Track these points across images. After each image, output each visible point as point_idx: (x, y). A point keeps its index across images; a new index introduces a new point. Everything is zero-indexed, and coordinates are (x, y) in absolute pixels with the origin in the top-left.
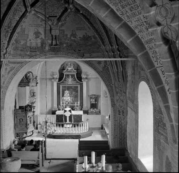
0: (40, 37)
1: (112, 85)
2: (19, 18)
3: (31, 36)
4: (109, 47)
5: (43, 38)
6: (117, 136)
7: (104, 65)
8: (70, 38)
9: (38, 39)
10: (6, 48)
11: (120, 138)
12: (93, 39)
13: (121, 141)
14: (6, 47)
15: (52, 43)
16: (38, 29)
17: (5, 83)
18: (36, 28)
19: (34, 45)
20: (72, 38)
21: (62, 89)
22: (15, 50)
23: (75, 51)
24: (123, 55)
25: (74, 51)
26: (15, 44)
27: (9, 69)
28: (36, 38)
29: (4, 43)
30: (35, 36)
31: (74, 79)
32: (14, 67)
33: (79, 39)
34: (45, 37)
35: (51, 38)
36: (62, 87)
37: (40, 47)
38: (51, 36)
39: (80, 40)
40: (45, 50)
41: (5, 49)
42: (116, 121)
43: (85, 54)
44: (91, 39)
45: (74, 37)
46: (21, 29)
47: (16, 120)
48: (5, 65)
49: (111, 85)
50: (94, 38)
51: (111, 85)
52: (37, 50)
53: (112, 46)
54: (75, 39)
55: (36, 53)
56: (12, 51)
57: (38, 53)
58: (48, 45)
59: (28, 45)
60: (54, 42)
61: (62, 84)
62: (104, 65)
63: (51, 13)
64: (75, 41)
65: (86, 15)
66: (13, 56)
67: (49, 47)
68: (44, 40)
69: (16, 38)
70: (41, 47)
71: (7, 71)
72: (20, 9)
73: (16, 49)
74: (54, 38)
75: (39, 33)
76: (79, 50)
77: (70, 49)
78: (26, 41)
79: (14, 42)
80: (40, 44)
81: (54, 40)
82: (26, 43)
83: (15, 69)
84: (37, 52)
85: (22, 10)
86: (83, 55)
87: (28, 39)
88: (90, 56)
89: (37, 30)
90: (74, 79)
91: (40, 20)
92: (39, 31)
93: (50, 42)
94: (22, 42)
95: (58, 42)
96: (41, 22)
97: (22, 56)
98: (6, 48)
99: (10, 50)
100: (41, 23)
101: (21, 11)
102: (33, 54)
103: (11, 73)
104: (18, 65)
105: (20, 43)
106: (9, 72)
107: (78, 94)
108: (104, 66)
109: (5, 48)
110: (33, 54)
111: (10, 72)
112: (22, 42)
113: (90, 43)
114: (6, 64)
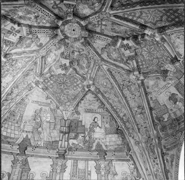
0: (179, 100)
2: (138, 92)
3: (170, 105)
9: (178, 103)
18: (166, 92)
22: (163, 131)
26: (159, 124)
28: (175, 103)
30: (171, 101)
46: (153, 102)
56: (161, 134)
59: (173, 116)
63: (159, 62)
65: (177, 20)
72: (131, 83)
75: (173, 94)
82: (170, 115)
85: (134, 83)
91: (161, 80)
94: (166, 117)
96: (165, 81)
100: (165, 83)
101: (135, 84)
105: (164, 119)
112: (166, 117)
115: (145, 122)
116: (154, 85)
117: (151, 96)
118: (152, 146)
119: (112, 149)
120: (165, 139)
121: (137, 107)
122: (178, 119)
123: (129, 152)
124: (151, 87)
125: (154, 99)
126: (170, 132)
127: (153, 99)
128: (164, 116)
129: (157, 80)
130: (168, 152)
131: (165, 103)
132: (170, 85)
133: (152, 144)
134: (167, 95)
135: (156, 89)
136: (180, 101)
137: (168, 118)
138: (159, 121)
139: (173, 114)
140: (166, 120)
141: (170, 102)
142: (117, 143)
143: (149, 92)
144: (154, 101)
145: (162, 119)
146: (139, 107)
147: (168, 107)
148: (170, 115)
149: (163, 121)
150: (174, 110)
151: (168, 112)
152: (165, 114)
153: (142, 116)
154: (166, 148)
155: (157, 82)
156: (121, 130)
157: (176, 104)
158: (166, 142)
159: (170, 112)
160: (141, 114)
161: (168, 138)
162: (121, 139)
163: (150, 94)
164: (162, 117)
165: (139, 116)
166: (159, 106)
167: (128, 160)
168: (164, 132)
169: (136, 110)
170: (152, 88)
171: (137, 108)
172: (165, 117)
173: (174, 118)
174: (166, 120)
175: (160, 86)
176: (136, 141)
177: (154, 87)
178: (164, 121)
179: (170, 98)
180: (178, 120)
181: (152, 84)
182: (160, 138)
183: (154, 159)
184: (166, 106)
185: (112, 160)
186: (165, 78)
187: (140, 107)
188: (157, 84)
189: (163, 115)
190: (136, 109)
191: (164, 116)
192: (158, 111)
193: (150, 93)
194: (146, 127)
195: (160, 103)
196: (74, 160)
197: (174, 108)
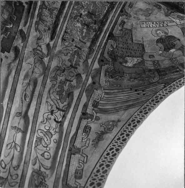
16: (167, 31)
28: (167, 49)
46: (121, 30)
78: (140, 59)
82: (143, 62)
89: (163, 32)
91: (162, 11)
92: (169, 34)
96: (167, 15)
98: (86, 61)
105: (126, 62)
116: (144, 11)
117: (126, 20)
118: (67, 85)
120: (107, 91)
121: (88, 12)
124: (135, 10)
125: (128, 26)
127: (125, 26)
129: (154, 8)
130: (98, 115)
131: (145, 44)
132: (174, 24)
134: (157, 34)
135: (143, 18)
143: (128, 13)
144: (124, 30)
146: (90, 14)
147: (148, 50)
149: (121, 63)
151: (142, 57)
153: (85, 30)
154: (99, 107)
155: (152, 10)
156: (24, 7)
159: (146, 58)
160: (86, 27)
161: (116, 91)
162: (6, 17)
163: (127, 16)
164: (123, 57)
165: (79, 25)
166: (130, 42)
169: (83, 14)
170: (136, 11)
171: (86, 13)
175: (152, 17)
177: (141, 13)
179: (160, 40)
181: (142, 8)
182: (97, 84)
183: (54, 108)
186: (171, 12)
187: (93, 17)
188: (150, 12)
189: (128, 56)
190: (84, 12)
192: (121, 46)
193: (128, 16)
195: (134, 39)
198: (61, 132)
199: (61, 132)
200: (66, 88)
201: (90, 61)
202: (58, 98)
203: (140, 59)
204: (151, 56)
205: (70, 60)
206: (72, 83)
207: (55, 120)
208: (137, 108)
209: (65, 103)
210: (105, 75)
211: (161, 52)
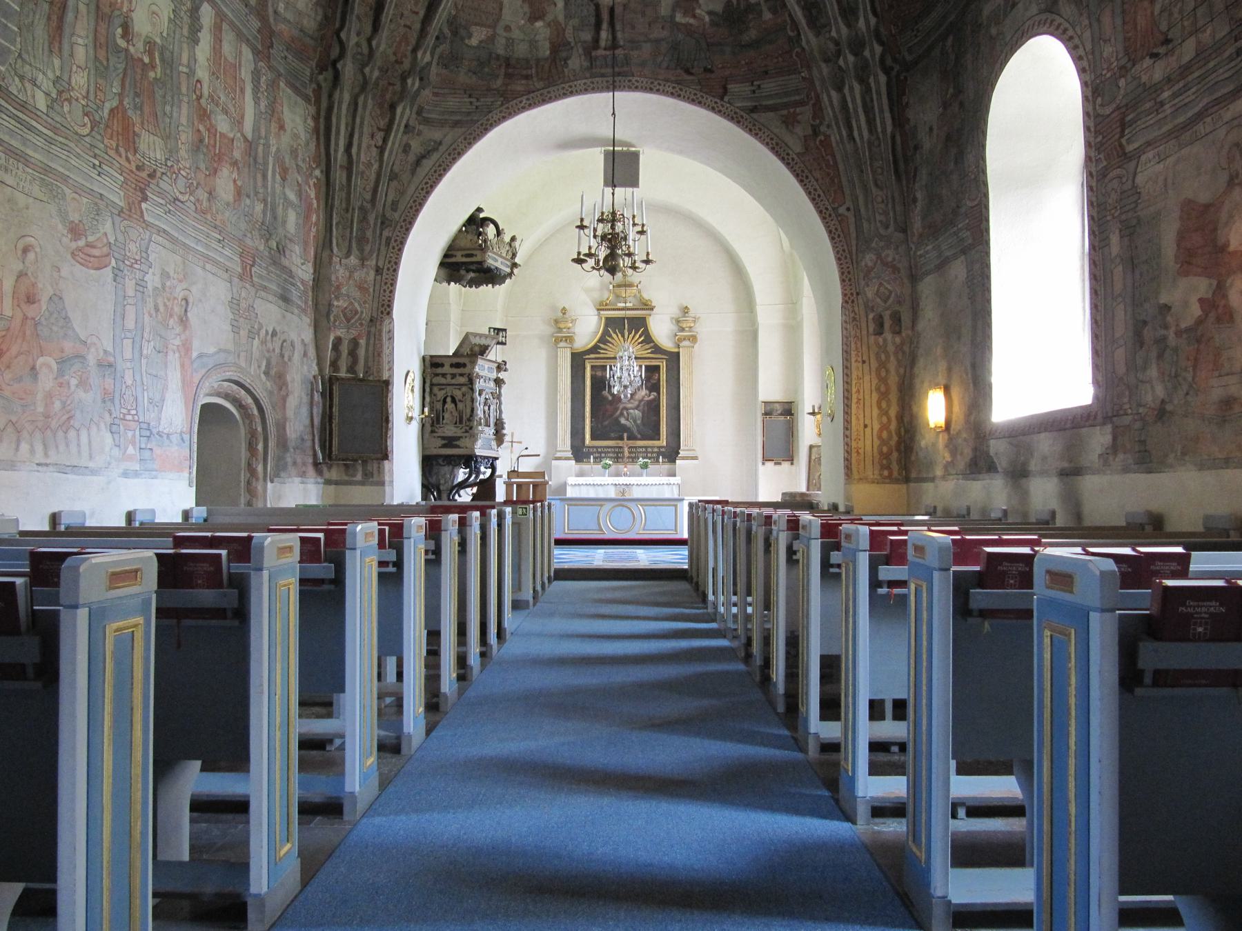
0: (549, 18)
1: (846, 213)
4: (838, 31)
5: (561, 18)
6: (868, 430)
7: (812, 125)
8: (672, 17)
9: (539, 24)
10: (415, 51)
11: (880, 437)
12: (767, 15)
13: (885, 449)
14: (413, 41)
15: (596, 40)
17: (401, 207)
19: (521, 50)
20: (679, 18)
21: (593, 377)
22: (446, 66)
23: (691, 74)
24: (895, 60)
25: (688, 72)
27: (416, 146)
29: (405, 26)
31: (642, 338)
32: (440, 143)
33: (707, 19)
34: (568, 16)
35: (593, 20)
36: (592, 367)
37: (546, 59)
38: (592, 8)
39: (714, 24)
40: (565, 70)
41: (409, 54)
42: (864, 362)
43: (729, 86)
44: (760, 13)
45: (685, 14)
47: (428, 399)
48: (402, 129)
49: (842, 210)
50: (769, 9)
51: (842, 210)
52: (534, 71)
53: (849, 26)
54: (692, 21)
55: (531, 82)
56: (434, 69)
57: (539, 85)
58: (581, 51)
60: (604, 35)
61: (592, 356)
62: (812, 125)
64: (688, 30)
66: (435, 94)
67: (583, 57)
68: (564, 30)
69: (453, 12)
70: (550, 61)
71: (412, 158)
73: (451, 61)
74: (605, 16)
76: (706, 70)
77: (667, 68)
78: (491, 32)
79: (446, 31)
80: (547, 45)
81: (605, 26)
82: (492, 39)
83: (442, 148)
84: (535, 79)
86: (721, 91)
87: (502, 24)
88: (754, 92)
90: (642, 338)
93: (587, 36)
94: (477, 36)
95: (619, 35)
97: (470, 96)
99: (428, 58)
102: (519, 86)
103: (428, 164)
104: (458, 131)
105: (470, 36)
106: (418, 162)
107: (658, 399)
108: (810, 132)
109: (410, 48)
110: (519, 88)
111: (425, 162)
112: (477, 36)
113: (753, 34)
114: (406, 126)
115: (416, 10)
119: (285, 34)
120: (436, 90)
122: (513, 62)
123: (320, 73)
126: (463, 78)
128: (474, 29)
130: (421, 127)
133: (394, 85)
136: (549, 25)
137: (481, 42)
138: (455, 33)
139: (503, 41)
140: (474, 42)
141: (522, 7)
142: (305, 22)
145: (463, 32)
148: (492, 39)
149: (462, 39)
150: (516, 34)
152: (482, 25)
154: (424, 115)
157: (532, 25)
158: (433, 98)
159: (500, 31)
161: (446, 91)
162: (319, 18)
167: (306, 99)
168: (444, 71)
172: (475, 34)
173: (501, 52)
174: (474, 42)
176: (359, 50)
178: (467, 41)
180: (508, 65)
183: (375, 128)
184: (501, 9)
185: (280, 75)
189: (476, 24)
191: (474, 29)
194: (410, 28)
196: (217, 14)
197: (520, 28)
198: (381, 161)
199: (381, 161)
200: (388, 96)
201: (419, 55)
202: (379, 113)
203: (491, 32)
204: (508, 29)
205: (395, 54)
206: (395, 87)
207: (375, 146)
208: (463, 130)
209: (387, 120)
210: (438, 64)
211: (523, 22)
